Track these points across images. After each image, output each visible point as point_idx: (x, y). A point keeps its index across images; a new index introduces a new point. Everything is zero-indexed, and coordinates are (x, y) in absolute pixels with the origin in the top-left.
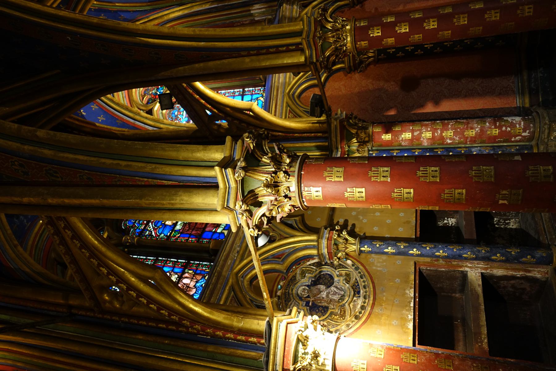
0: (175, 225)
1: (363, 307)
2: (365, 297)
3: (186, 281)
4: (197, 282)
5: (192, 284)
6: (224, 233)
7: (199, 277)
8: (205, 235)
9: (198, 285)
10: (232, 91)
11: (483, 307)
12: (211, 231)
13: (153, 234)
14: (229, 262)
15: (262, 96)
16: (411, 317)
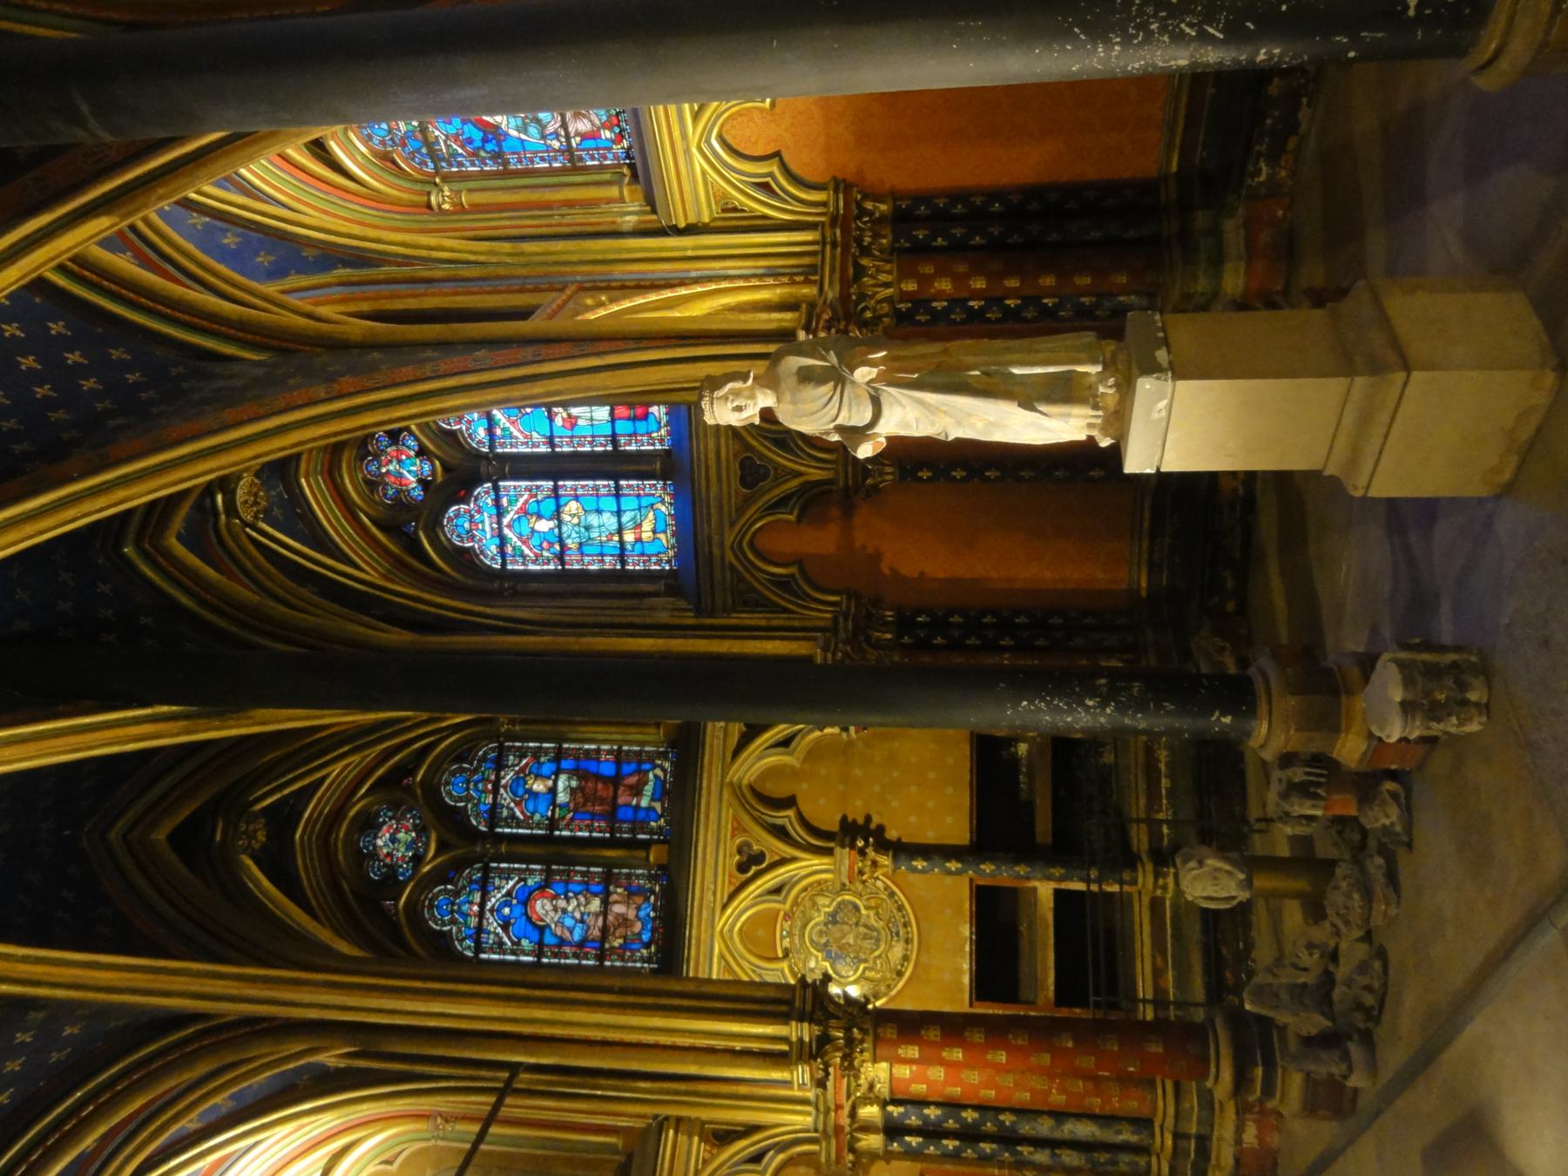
0: (553, 791)
1: (906, 958)
2: (907, 941)
3: (618, 909)
4: (638, 909)
5: (631, 914)
6: (653, 809)
7: (639, 900)
8: (621, 813)
9: (642, 914)
10: (591, 483)
11: (1052, 941)
12: (628, 805)
13: (518, 814)
14: (705, 914)
15: (663, 502)
16: (966, 966)
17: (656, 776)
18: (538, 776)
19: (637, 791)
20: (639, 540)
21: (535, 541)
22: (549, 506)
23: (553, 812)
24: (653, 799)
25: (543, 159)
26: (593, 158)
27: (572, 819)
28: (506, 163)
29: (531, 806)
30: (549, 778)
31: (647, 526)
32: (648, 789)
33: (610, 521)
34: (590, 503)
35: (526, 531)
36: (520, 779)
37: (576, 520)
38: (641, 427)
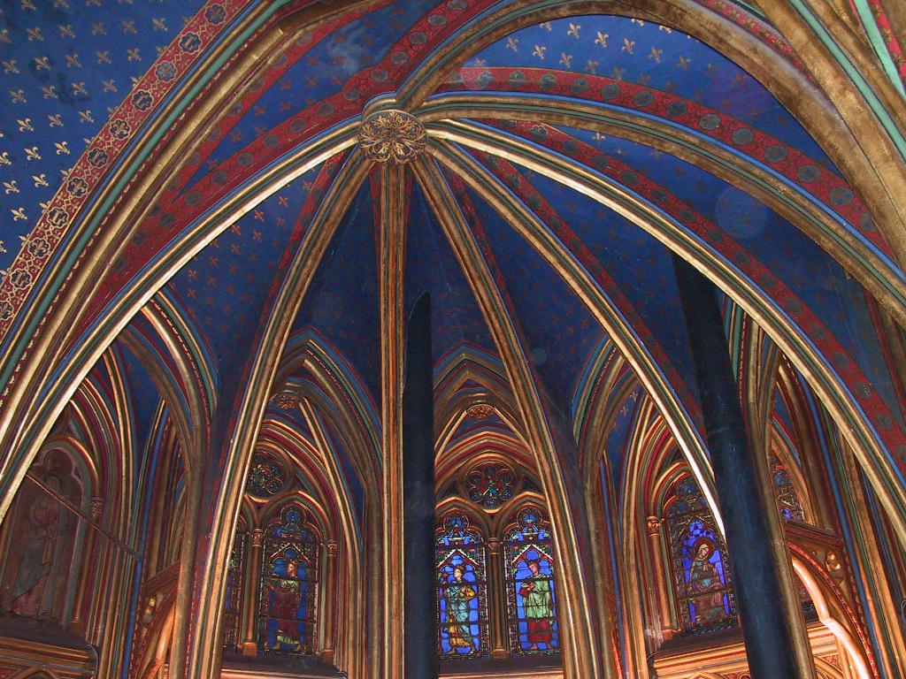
6: (275, 645)
17: (297, 645)
18: (297, 567)
19: (286, 633)
20: (451, 635)
21: (448, 569)
22: (470, 577)
23: (275, 577)
24: (281, 643)
25: (680, 581)
26: (684, 610)
27: (270, 589)
28: (675, 557)
29: (279, 562)
30: (296, 575)
31: (460, 641)
32: (289, 641)
33: (463, 616)
34: (473, 604)
35: (454, 563)
36: (295, 556)
37: (462, 595)
38: (524, 638)
